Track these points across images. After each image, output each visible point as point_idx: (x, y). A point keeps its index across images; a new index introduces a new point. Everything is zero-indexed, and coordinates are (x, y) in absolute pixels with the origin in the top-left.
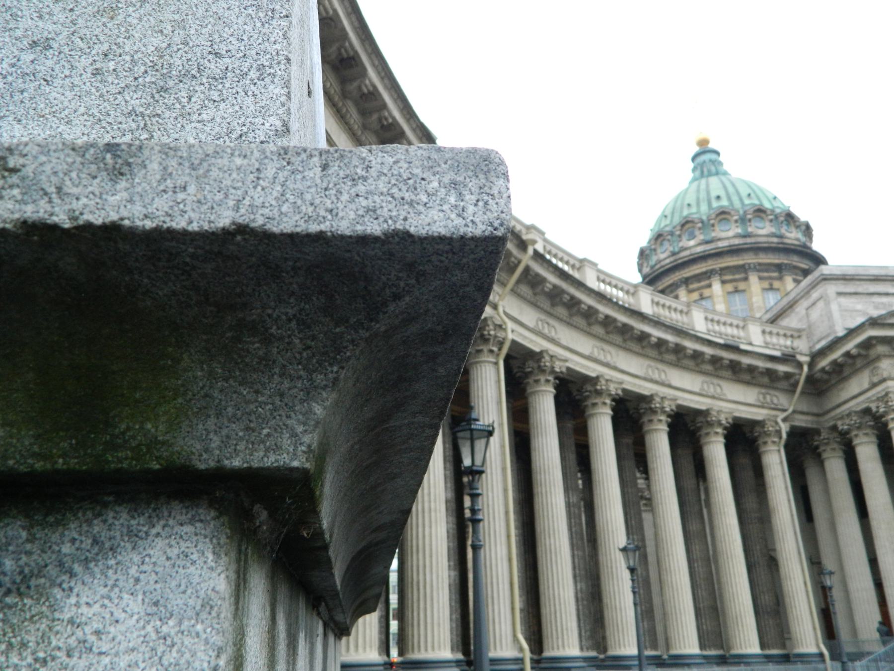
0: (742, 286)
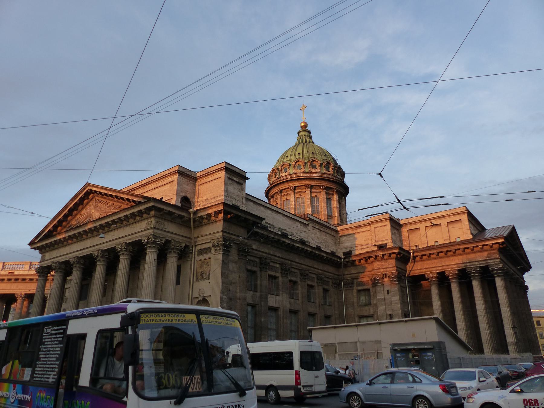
0: (303, 195)
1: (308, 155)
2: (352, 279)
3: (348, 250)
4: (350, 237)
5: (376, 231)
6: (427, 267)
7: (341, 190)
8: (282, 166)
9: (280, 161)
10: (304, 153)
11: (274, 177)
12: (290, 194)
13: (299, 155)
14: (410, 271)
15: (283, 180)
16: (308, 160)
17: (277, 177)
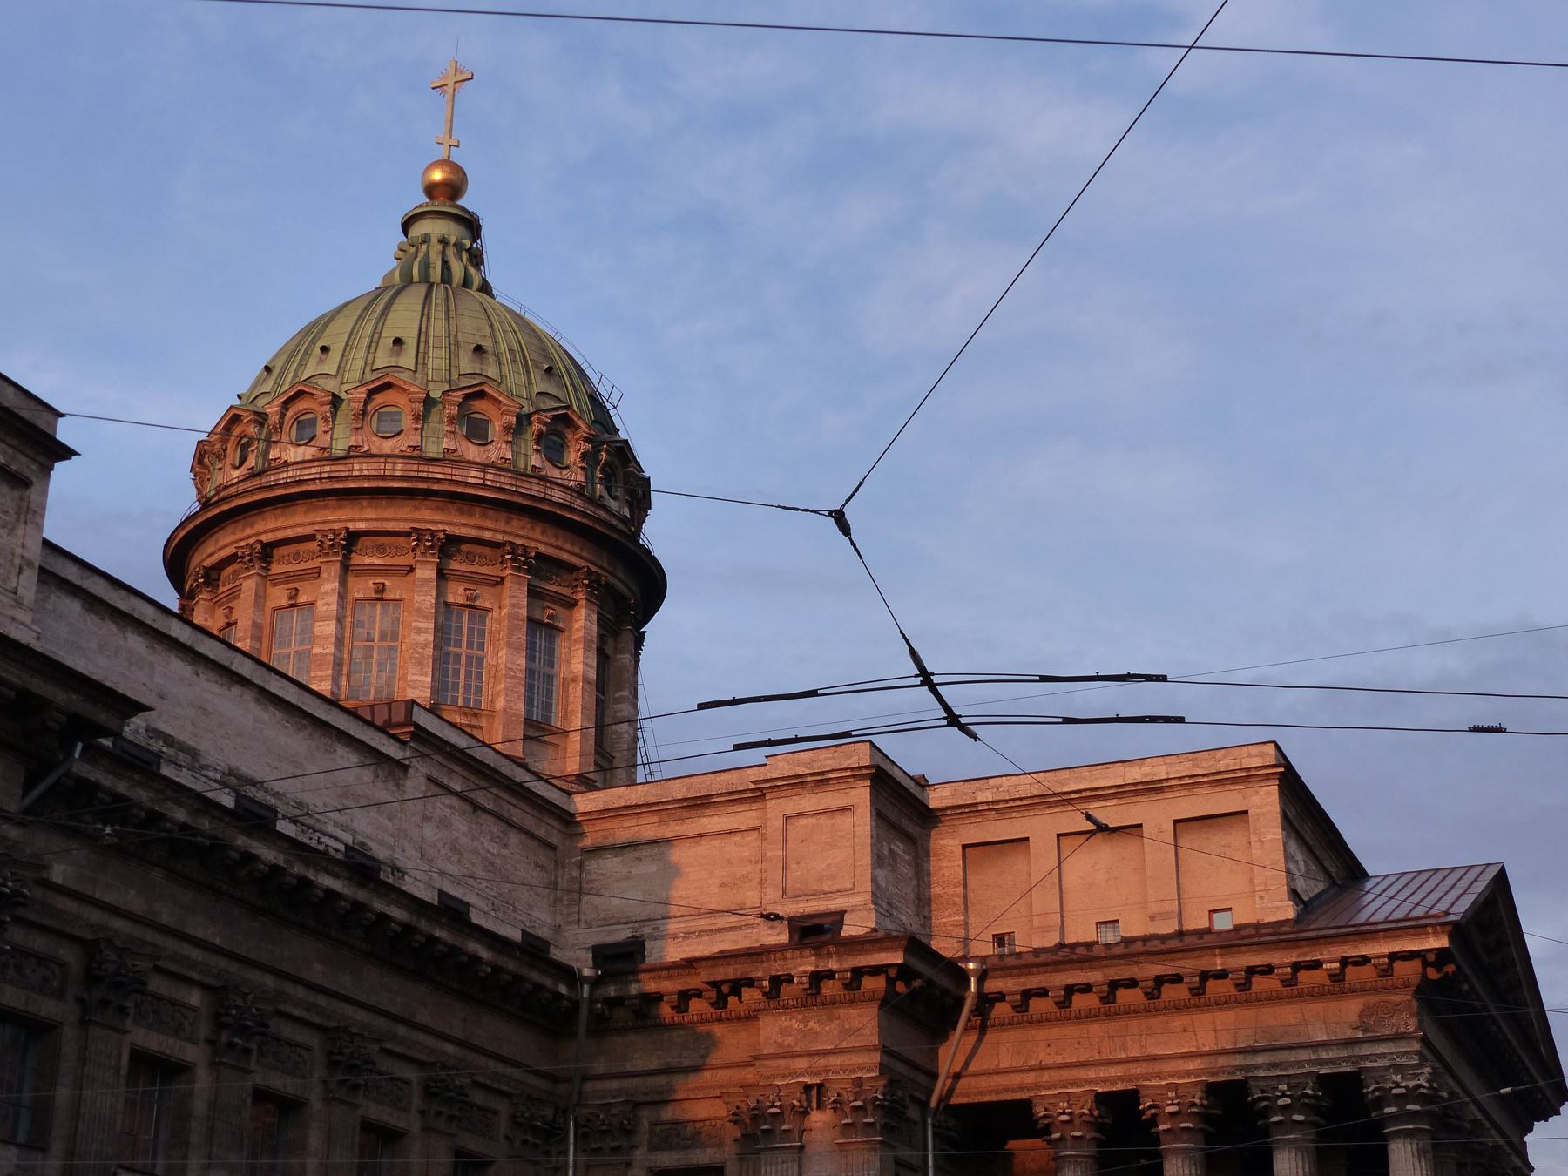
1: (452, 355)
2: (627, 1102)
3: (623, 934)
4: (640, 859)
5: (791, 836)
6: (1049, 1061)
7: (619, 585)
8: (286, 404)
9: (276, 372)
10: (427, 342)
11: (229, 461)
12: (316, 574)
13: (398, 354)
14: (957, 1077)
15: (286, 484)
16: (447, 387)
17: (251, 462)
